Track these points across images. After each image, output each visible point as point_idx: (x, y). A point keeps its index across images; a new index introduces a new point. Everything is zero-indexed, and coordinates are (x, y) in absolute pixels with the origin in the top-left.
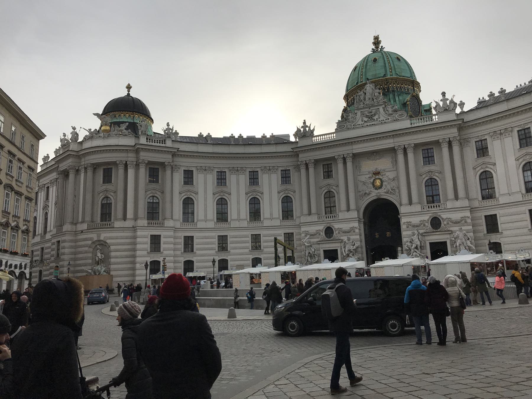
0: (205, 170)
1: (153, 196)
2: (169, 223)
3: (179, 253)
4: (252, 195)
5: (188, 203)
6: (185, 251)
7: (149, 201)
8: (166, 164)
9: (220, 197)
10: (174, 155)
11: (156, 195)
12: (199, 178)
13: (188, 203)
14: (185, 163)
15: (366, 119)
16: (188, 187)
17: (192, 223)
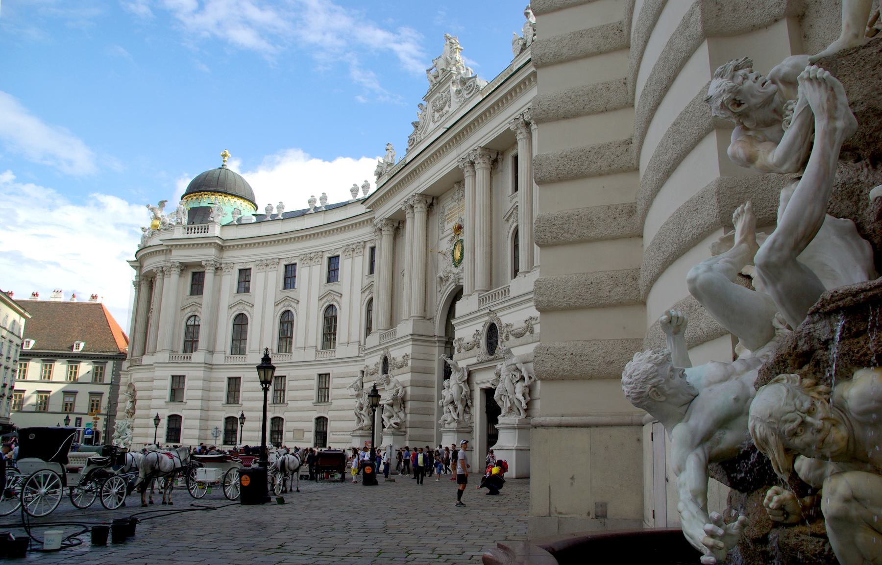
0: (267, 265)
1: (195, 316)
2: (198, 356)
3: (219, 404)
4: (327, 301)
5: (241, 321)
6: (228, 402)
7: (189, 323)
8: (204, 263)
9: (284, 309)
10: (221, 248)
11: (196, 314)
12: (257, 279)
13: (241, 321)
14: (240, 258)
15: (437, 115)
16: (243, 297)
17: (241, 356)
